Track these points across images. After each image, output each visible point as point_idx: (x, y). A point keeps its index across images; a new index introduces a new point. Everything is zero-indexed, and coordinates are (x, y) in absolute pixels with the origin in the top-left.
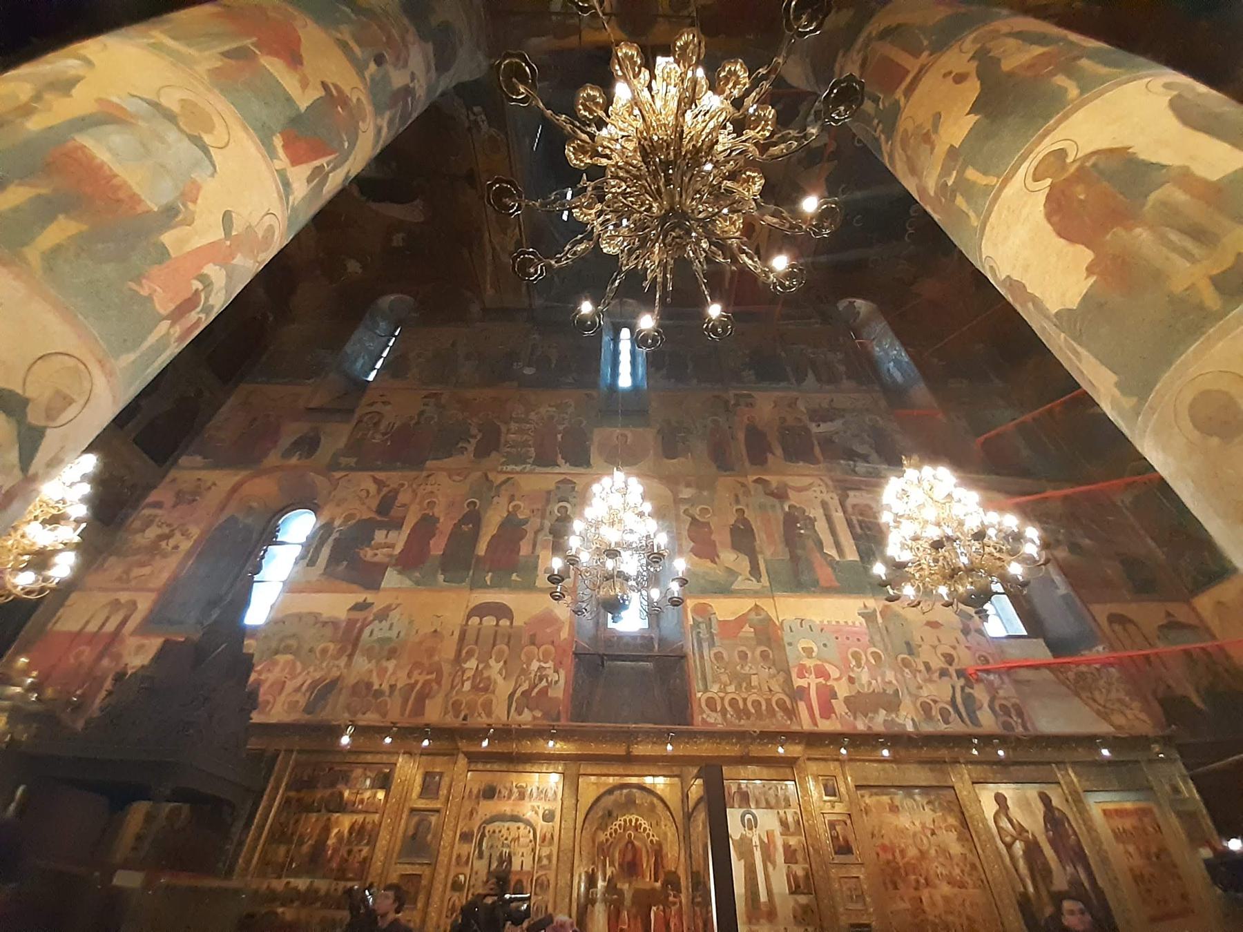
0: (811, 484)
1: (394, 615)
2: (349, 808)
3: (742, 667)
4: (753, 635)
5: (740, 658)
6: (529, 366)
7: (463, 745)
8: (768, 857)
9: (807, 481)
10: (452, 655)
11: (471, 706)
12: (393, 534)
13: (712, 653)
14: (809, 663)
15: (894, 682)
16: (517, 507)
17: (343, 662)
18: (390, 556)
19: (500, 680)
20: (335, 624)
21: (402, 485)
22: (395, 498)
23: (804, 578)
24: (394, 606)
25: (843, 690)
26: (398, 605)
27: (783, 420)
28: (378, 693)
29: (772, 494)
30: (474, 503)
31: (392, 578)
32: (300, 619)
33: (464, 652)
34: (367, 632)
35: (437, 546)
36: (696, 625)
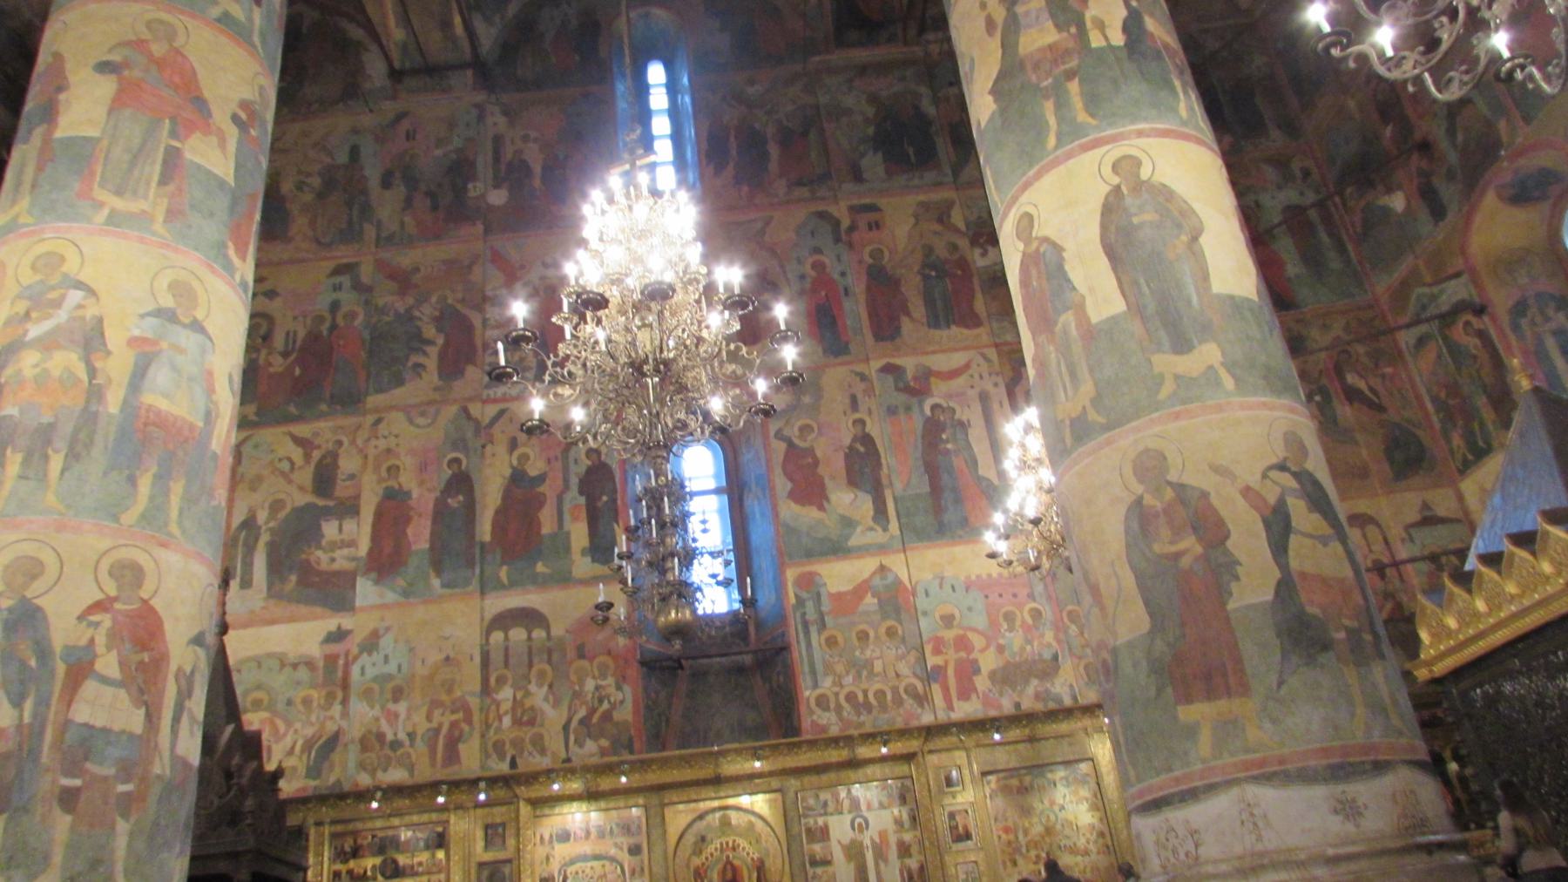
0: (967, 366)
1: (386, 642)
2: (408, 871)
3: (862, 653)
4: (877, 608)
5: (859, 639)
6: (496, 187)
7: (522, 791)
8: (880, 854)
9: (958, 359)
10: (477, 687)
11: (517, 744)
12: (349, 525)
13: (823, 638)
14: (949, 635)
15: (1054, 644)
16: (524, 458)
17: (337, 709)
18: (354, 559)
19: (547, 708)
20: (310, 664)
21: (340, 443)
22: (335, 466)
23: (950, 516)
24: (381, 632)
25: (988, 662)
26: (388, 629)
27: (929, 250)
28: (396, 745)
29: (907, 390)
30: (457, 461)
31: (366, 591)
32: (260, 665)
33: (493, 680)
34: (355, 670)
35: (420, 535)
36: (800, 602)
